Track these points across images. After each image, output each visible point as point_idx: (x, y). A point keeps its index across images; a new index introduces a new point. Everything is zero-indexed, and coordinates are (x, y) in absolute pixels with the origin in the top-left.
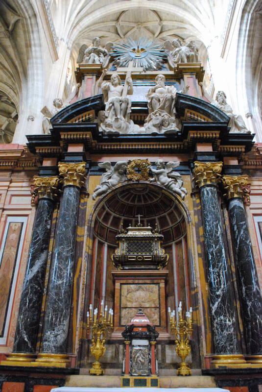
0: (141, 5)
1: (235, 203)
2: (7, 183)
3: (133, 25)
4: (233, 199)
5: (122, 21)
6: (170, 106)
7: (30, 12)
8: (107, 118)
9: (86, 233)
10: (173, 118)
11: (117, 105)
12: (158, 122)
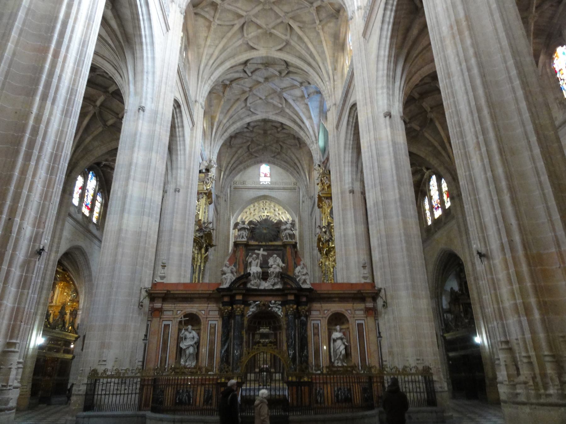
0: (269, 55)
2: (207, 305)
3: (260, 66)
4: (302, 316)
6: (278, 275)
7: (180, 124)
8: (251, 281)
9: (244, 332)
10: (279, 280)
11: (256, 275)
12: (273, 283)
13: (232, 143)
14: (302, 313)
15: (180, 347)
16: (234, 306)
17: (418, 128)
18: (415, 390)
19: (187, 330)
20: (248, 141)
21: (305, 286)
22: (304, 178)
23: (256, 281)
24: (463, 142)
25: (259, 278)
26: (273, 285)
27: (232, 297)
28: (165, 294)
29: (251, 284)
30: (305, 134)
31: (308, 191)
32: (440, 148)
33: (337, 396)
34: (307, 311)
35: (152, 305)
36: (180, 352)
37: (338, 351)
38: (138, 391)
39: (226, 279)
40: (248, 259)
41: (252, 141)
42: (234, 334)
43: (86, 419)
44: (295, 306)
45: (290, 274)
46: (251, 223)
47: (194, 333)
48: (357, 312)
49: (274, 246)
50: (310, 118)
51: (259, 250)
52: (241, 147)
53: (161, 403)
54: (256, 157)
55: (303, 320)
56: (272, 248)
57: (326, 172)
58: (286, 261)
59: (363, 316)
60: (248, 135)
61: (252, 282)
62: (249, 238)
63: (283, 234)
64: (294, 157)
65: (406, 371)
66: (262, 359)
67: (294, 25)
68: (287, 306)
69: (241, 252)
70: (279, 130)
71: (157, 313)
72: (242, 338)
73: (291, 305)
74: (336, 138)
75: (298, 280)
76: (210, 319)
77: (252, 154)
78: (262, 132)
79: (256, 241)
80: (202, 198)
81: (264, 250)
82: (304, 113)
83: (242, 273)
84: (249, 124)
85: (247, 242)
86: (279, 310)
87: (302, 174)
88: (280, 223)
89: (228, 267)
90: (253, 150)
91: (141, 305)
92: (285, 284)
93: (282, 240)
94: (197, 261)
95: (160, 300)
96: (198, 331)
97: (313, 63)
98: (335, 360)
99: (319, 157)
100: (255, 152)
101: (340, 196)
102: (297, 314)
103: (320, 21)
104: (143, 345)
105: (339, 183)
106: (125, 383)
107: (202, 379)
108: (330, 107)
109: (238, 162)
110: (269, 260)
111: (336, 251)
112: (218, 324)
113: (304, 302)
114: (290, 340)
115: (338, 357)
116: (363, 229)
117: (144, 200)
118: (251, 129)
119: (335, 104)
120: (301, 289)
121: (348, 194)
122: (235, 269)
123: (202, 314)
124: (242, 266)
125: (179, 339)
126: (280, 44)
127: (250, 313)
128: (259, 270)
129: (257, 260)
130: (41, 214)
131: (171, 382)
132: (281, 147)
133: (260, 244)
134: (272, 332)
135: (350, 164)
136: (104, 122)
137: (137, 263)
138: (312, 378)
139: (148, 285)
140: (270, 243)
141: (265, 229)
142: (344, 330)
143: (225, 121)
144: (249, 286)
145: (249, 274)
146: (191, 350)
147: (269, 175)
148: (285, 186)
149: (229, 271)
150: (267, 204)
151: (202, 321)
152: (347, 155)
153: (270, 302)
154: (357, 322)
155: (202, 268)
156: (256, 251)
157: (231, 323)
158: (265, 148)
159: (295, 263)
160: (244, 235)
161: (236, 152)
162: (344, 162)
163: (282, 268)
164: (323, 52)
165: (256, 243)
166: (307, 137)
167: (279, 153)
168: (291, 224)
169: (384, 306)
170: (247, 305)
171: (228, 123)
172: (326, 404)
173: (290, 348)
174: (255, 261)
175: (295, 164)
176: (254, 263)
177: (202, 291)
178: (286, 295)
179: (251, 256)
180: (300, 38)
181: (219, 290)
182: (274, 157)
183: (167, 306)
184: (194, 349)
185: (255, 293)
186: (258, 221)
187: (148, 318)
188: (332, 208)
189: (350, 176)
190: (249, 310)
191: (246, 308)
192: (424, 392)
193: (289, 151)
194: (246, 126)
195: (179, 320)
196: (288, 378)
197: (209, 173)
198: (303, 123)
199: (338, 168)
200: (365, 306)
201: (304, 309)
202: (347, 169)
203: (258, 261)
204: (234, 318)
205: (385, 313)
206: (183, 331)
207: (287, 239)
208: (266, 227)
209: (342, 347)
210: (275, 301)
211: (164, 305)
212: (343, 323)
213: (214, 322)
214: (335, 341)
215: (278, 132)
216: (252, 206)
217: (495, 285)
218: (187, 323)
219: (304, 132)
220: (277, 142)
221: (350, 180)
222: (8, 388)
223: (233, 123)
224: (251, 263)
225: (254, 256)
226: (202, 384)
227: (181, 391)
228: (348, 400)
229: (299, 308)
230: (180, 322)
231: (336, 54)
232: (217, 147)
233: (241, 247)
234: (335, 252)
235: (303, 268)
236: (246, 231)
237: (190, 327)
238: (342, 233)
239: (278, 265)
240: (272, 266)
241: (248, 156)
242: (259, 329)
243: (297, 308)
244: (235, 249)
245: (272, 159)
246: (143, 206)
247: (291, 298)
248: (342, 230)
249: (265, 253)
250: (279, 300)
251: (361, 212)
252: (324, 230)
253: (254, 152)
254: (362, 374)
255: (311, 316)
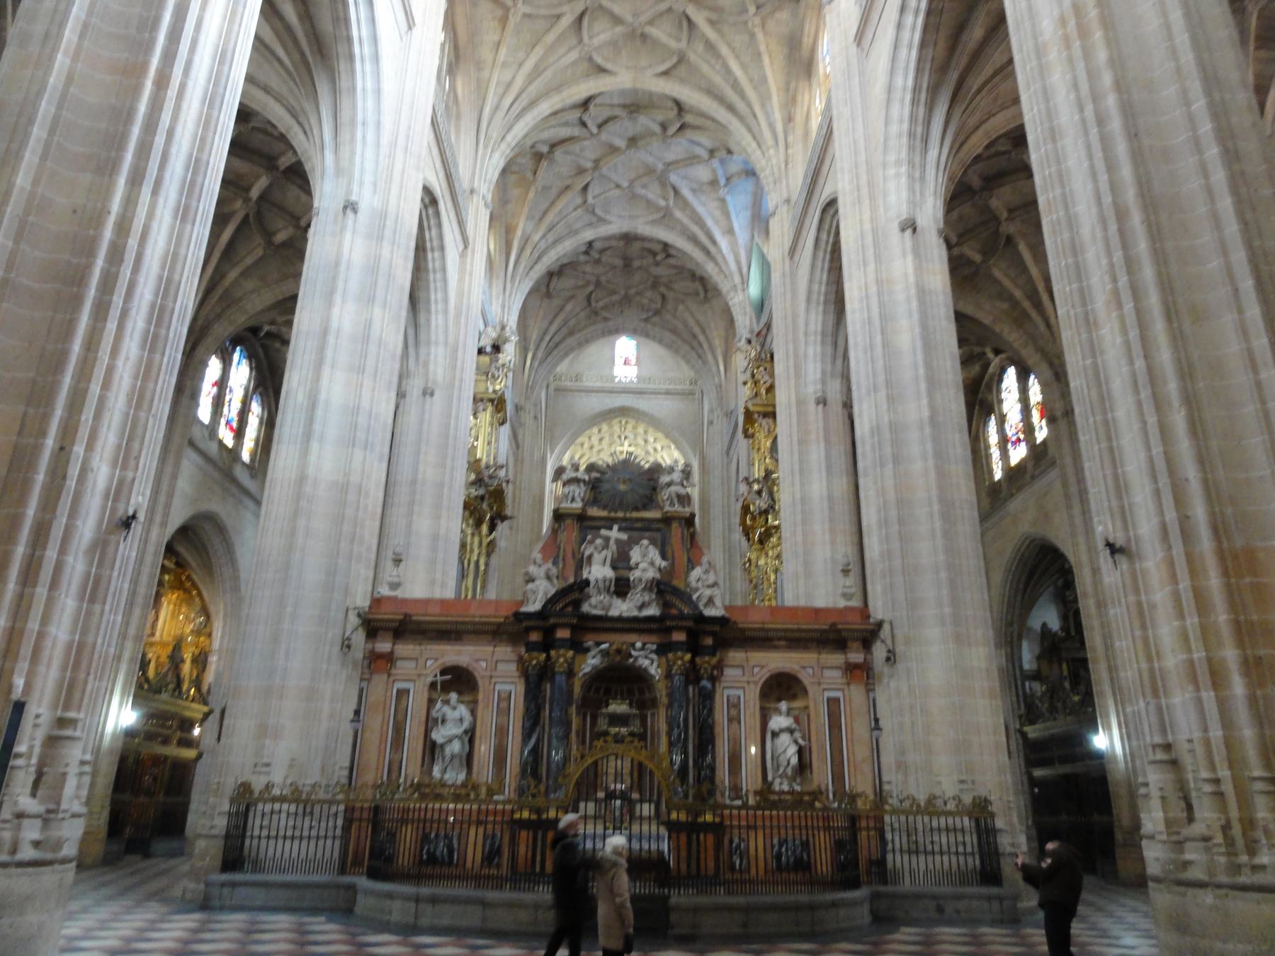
0: (639, 86)
1: (705, 683)
2: (491, 649)
3: (618, 112)
5: (595, 105)
6: (651, 586)
7: (435, 243)
10: (654, 596)
12: (639, 604)
13: (552, 286)
14: (702, 671)
15: (431, 740)
16: (553, 653)
17: (978, 258)
18: (953, 849)
19: (447, 702)
20: (588, 283)
21: (710, 612)
22: (714, 369)
23: (602, 597)
24: (1077, 266)
25: (608, 591)
26: (642, 607)
27: (549, 632)
28: (402, 622)
29: (590, 605)
30: (717, 270)
31: (722, 398)
32: (1026, 304)
33: (778, 857)
34: (714, 668)
35: (370, 646)
36: (432, 750)
37: (782, 758)
38: (339, 832)
39: (534, 593)
40: (585, 549)
41: (598, 284)
42: (550, 713)
43: (226, 891)
44: (688, 657)
45: (676, 583)
46: (591, 468)
47: (463, 710)
48: (827, 673)
49: (642, 520)
50: (730, 231)
51: (611, 529)
52: (572, 297)
53: (390, 859)
54: (606, 319)
55: (704, 688)
56: (639, 525)
57: (763, 355)
58: (669, 554)
59: (840, 681)
60: (588, 269)
61: (593, 601)
62: (587, 503)
63: (664, 495)
64: (691, 322)
65: (934, 806)
66: (613, 771)
67: (699, 18)
68: (670, 655)
69: (570, 534)
70: (659, 258)
71: (381, 663)
72: (569, 724)
73: (680, 653)
74: (788, 280)
75: (695, 597)
76: (500, 680)
77: (596, 313)
78: (618, 262)
79: (604, 508)
80: (484, 410)
81: (620, 529)
82: (717, 222)
83: (571, 580)
84: (590, 244)
85: (584, 509)
86: (652, 663)
87: (710, 357)
88: (657, 469)
89: (540, 566)
90: (601, 304)
91: (346, 645)
92: (666, 605)
93: (662, 508)
94: (472, 551)
95: (390, 635)
96: (471, 706)
97: (740, 105)
98: (774, 779)
99: (748, 322)
100: (605, 308)
101: (794, 410)
102: (692, 675)
103: (758, 8)
104: (351, 733)
105: (792, 382)
106: (312, 813)
107: (479, 811)
108: (777, 207)
109: (565, 330)
110: (632, 553)
111: (783, 534)
112: (517, 690)
113: (708, 647)
114: (676, 731)
115: (781, 770)
116: (845, 486)
117: (356, 410)
118: (597, 256)
119: (788, 201)
120: (701, 619)
121: (812, 406)
122: (554, 571)
123: (481, 670)
124: (571, 564)
125: (431, 723)
126: (663, 61)
127: (587, 669)
128: (609, 573)
129: (605, 552)
130: (130, 440)
131: (411, 814)
132: (663, 297)
133: (613, 514)
134: (634, 711)
135: (819, 338)
136: (268, 235)
137: (338, 553)
138: (722, 816)
139: (362, 601)
140: (635, 515)
141: (624, 482)
142: (796, 713)
143: (536, 238)
144: (586, 608)
145: (587, 583)
146: (456, 747)
147: (633, 361)
148: (671, 387)
149: (542, 574)
150: (630, 427)
151: (480, 683)
152: (813, 317)
153: (633, 645)
154: (827, 694)
155: (482, 568)
156: (603, 532)
157: (545, 690)
158: (627, 300)
159: (689, 560)
160: (576, 494)
161: (562, 309)
162: (806, 334)
163: (660, 569)
164: (764, 80)
165: (604, 513)
166: (722, 276)
167: (657, 313)
168: (683, 471)
169: (888, 659)
170: (581, 650)
171: (543, 241)
172: (753, 871)
173: (675, 749)
174: (600, 552)
175: (694, 336)
176: (598, 557)
177: (481, 617)
178: (668, 631)
179: (591, 542)
180: (710, 46)
181: (519, 617)
182: (646, 320)
183: (404, 649)
184: (463, 744)
185: (600, 625)
186: (608, 466)
187: (362, 673)
188: (776, 438)
189: (819, 365)
190: (585, 661)
191: (579, 658)
192: (973, 854)
193: (681, 307)
194: (583, 249)
195: (430, 679)
196: (669, 814)
197: (500, 355)
198: (714, 242)
199: (791, 347)
200: (847, 659)
201: (708, 663)
202: (811, 351)
203: (608, 554)
204: (552, 679)
205: (891, 676)
206: (439, 705)
207: (672, 504)
208: (627, 477)
209: (792, 750)
210: (644, 644)
211: (396, 647)
212: (793, 697)
213: (507, 687)
214: (775, 735)
215: (657, 264)
216: (595, 430)
217: (1143, 616)
218: (446, 687)
219: (717, 264)
220: (655, 285)
221: (819, 376)
222: (61, 816)
223: (557, 241)
224: (590, 557)
225: (599, 541)
226: (479, 823)
227: (433, 835)
228: (802, 865)
229: (698, 660)
230: (433, 686)
231: (793, 85)
232: (519, 296)
233: (569, 521)
234: (779, 538)
235: (706, 572)
236: (582, 484)
237: (453, 696)
238: (798, 496)
239: (652, 564)
240: (637, 564)
241: (588, 317)
242: (607, 705)
243: (692, 661)
244: (556, 526)
245: (642, 324)
246: (354, 427)
247: (680, 637)
248: (798, 487)
249: (624, 536)
250: (653, 642)
251: (842, 448)
252: (756, 487)
253: (602, 309)
254: (835, 810)
255: (723, 679)
